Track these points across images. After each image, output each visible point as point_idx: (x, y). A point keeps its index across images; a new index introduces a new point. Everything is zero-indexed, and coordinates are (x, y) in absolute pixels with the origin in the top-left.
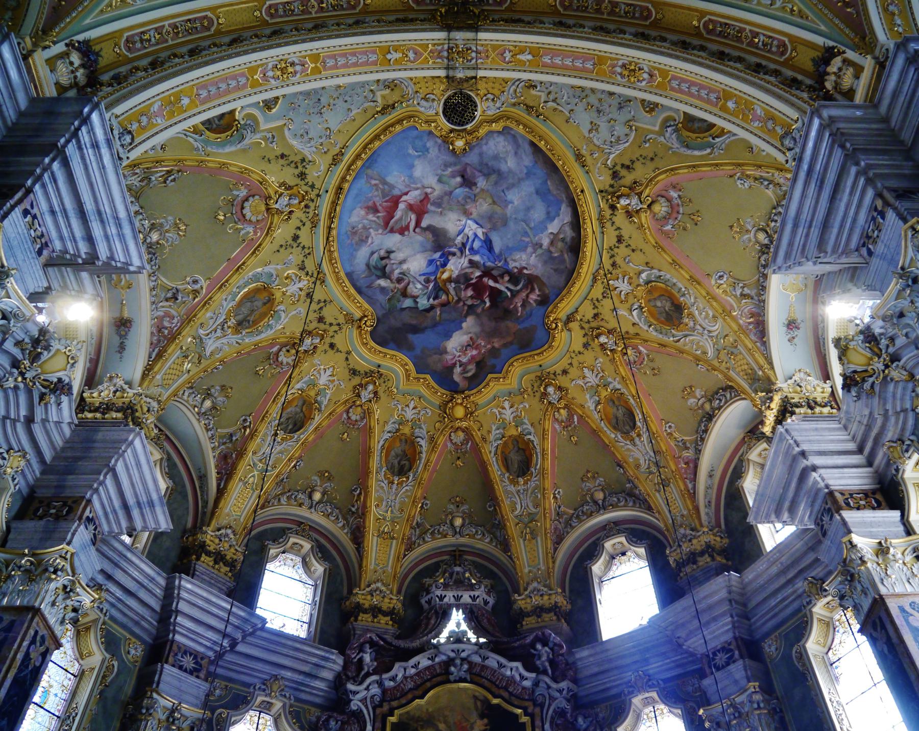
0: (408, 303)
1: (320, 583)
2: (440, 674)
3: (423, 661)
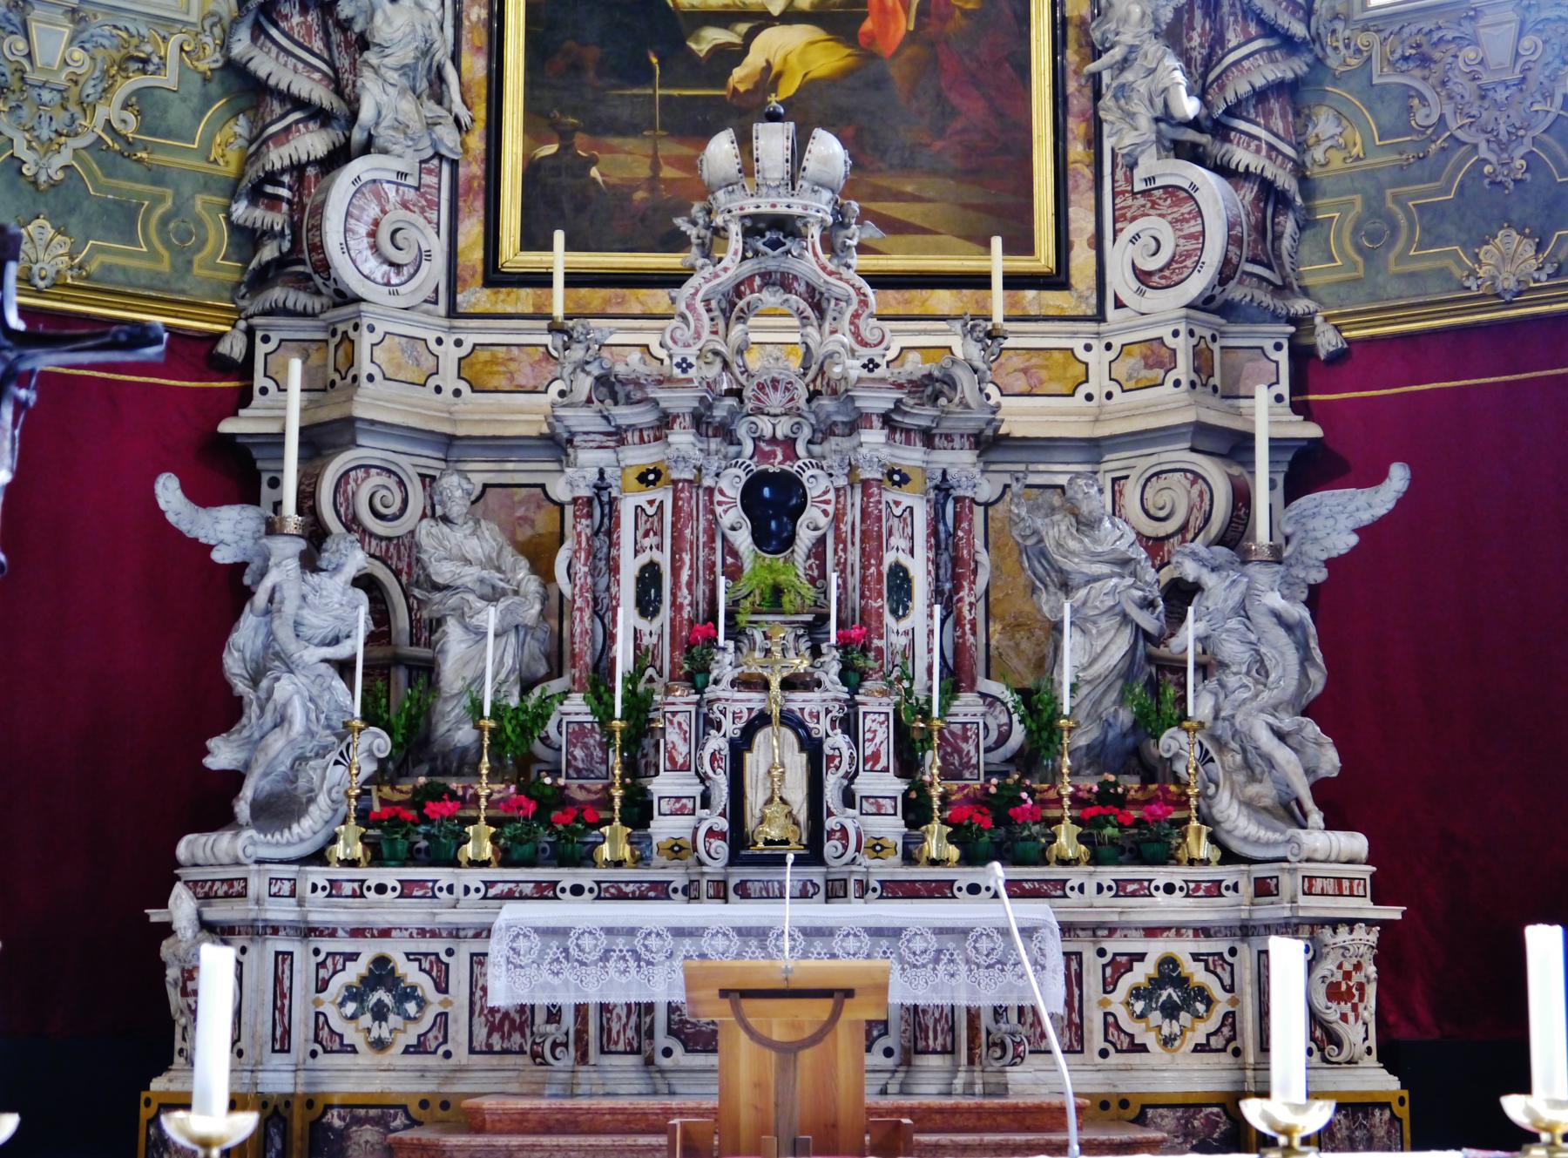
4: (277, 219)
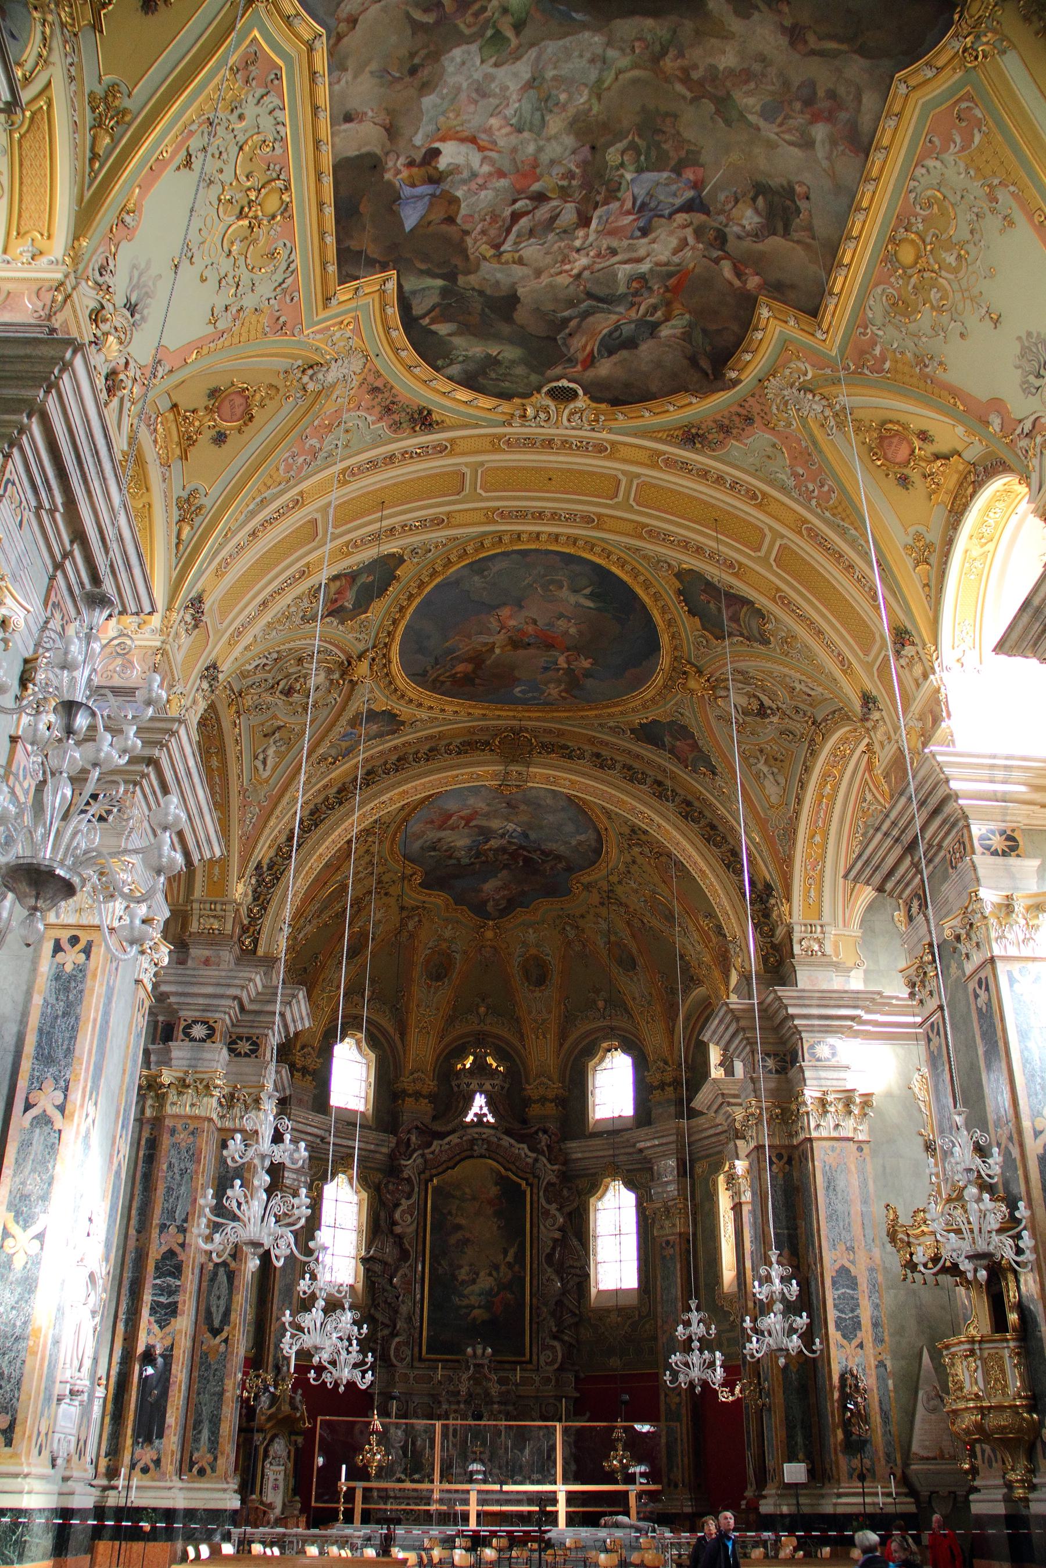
0: (453, 861)
2: (466, 1153)
3: (454, 1139)
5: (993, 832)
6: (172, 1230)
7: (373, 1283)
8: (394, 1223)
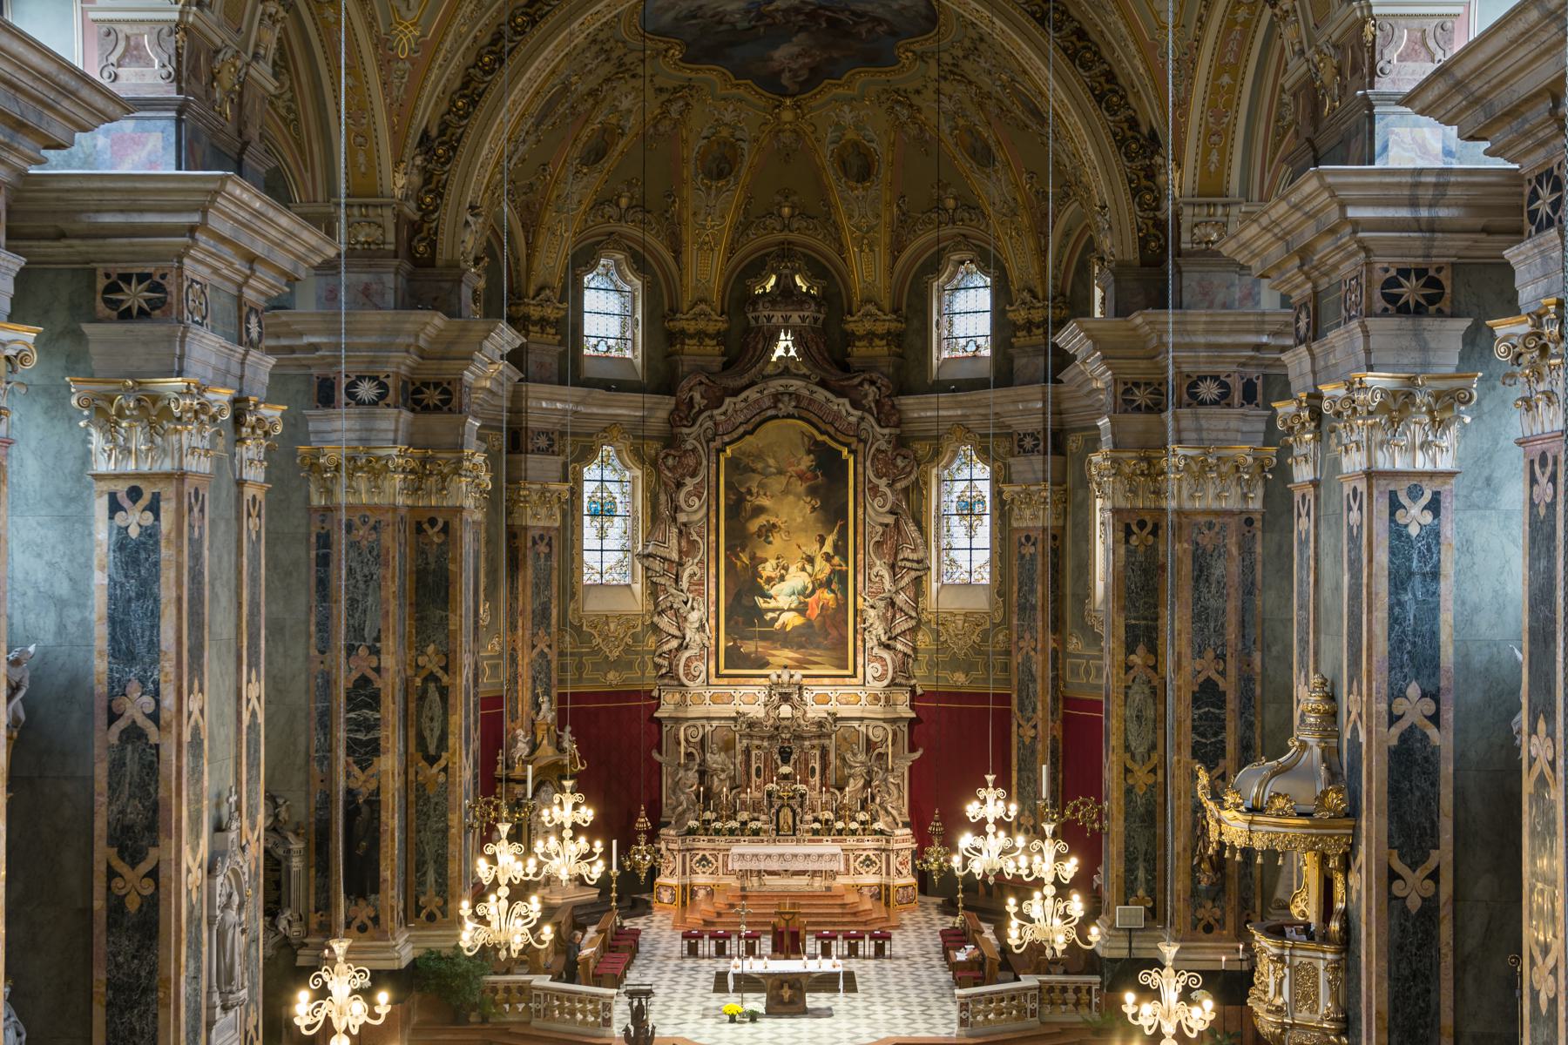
0: (723, 28)
1: (639, 294)
3: (752, 394)
4: (666, 663)
5: (1404, 273)
6: (363, 651)
7: (655, 584)
8: (677, 509)
